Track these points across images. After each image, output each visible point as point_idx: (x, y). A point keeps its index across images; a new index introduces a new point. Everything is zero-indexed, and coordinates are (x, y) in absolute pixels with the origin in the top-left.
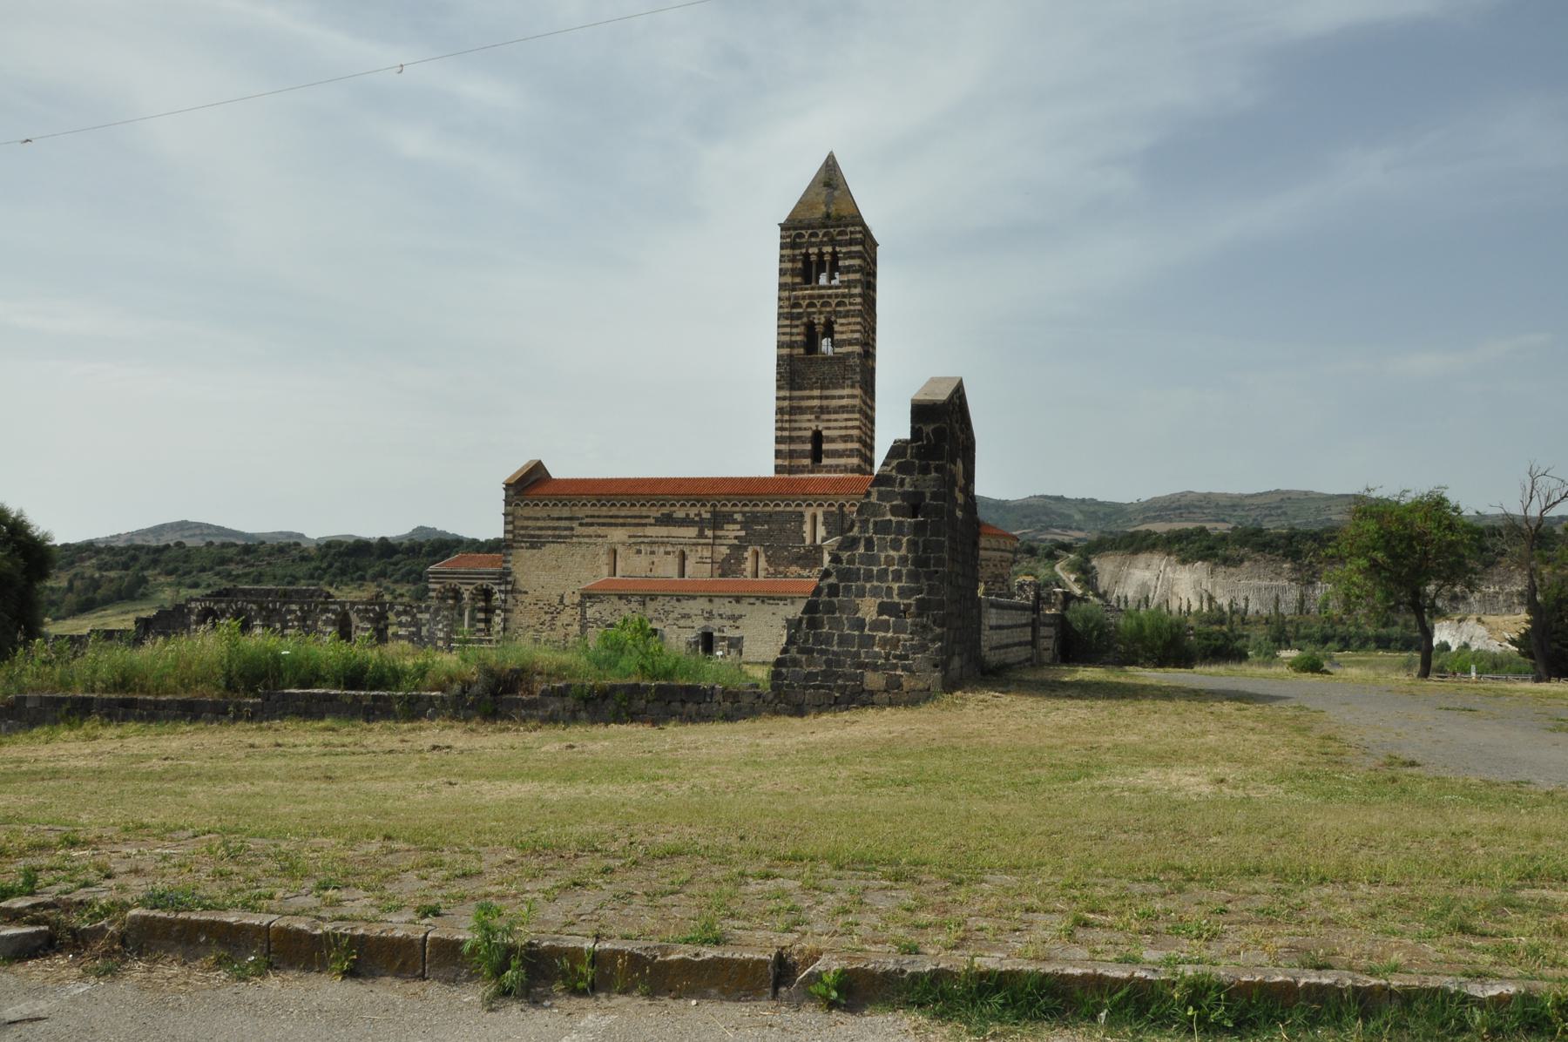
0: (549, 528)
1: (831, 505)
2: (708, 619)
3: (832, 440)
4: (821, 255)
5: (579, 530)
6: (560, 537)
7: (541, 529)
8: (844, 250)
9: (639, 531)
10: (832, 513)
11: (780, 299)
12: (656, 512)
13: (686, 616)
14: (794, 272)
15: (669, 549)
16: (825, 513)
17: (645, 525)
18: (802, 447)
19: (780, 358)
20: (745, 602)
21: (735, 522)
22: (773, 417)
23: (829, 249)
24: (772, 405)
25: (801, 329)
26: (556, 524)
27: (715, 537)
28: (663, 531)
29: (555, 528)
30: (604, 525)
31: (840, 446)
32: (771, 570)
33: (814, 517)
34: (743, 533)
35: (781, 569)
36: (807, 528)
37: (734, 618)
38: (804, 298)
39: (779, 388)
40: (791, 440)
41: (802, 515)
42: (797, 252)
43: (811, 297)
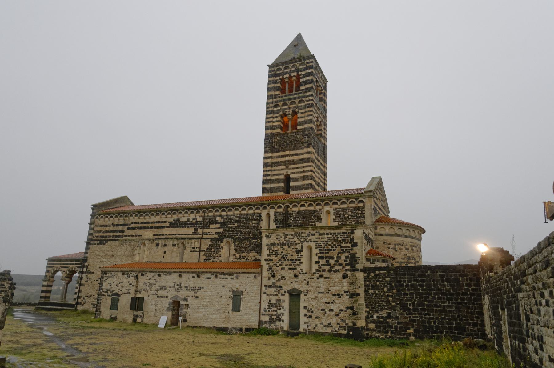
0: (111, 231)
1: (280, 207)
2: (177, 290)
3: (296, 180)
4: (291, 77)
5: (128, 232)
6: (116, 236)
7: (107, 232)
8: (303, 73)
9: (160, 231)
10: (280, 213)
11: (267, 104)
12: (170, 218)
13: (163, 288)
14: (276, 89)
15: (175, 242)
16: (276, 213)
17: (163, 227)
18: (279, 183)
19: (266, 135)
20: (203, 277)
21: (216, 223)
22: (262, 169)
23: (295, 74)
24: (261, 162)
25: (279, 118)
26: (115, 228)
27: (203, 233)
28: (174, 231)
29: (114, 231)
30: (141, 228)
31: (300, 183)
32: (238, 256)
33: (268, 215)
34: (221, 230)
35: (244, 255)
36: (264, 224)
37: (196, 289)
38: (280, 101)
39: (266, 152)
40: (272, 181)
41: (260, 216)
42: (278, 78)
43: (284, 100)
